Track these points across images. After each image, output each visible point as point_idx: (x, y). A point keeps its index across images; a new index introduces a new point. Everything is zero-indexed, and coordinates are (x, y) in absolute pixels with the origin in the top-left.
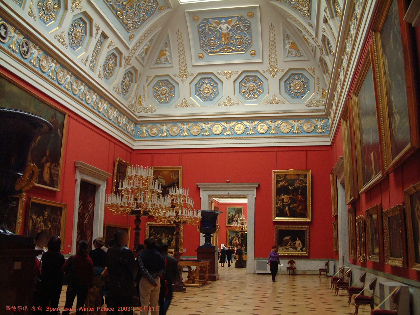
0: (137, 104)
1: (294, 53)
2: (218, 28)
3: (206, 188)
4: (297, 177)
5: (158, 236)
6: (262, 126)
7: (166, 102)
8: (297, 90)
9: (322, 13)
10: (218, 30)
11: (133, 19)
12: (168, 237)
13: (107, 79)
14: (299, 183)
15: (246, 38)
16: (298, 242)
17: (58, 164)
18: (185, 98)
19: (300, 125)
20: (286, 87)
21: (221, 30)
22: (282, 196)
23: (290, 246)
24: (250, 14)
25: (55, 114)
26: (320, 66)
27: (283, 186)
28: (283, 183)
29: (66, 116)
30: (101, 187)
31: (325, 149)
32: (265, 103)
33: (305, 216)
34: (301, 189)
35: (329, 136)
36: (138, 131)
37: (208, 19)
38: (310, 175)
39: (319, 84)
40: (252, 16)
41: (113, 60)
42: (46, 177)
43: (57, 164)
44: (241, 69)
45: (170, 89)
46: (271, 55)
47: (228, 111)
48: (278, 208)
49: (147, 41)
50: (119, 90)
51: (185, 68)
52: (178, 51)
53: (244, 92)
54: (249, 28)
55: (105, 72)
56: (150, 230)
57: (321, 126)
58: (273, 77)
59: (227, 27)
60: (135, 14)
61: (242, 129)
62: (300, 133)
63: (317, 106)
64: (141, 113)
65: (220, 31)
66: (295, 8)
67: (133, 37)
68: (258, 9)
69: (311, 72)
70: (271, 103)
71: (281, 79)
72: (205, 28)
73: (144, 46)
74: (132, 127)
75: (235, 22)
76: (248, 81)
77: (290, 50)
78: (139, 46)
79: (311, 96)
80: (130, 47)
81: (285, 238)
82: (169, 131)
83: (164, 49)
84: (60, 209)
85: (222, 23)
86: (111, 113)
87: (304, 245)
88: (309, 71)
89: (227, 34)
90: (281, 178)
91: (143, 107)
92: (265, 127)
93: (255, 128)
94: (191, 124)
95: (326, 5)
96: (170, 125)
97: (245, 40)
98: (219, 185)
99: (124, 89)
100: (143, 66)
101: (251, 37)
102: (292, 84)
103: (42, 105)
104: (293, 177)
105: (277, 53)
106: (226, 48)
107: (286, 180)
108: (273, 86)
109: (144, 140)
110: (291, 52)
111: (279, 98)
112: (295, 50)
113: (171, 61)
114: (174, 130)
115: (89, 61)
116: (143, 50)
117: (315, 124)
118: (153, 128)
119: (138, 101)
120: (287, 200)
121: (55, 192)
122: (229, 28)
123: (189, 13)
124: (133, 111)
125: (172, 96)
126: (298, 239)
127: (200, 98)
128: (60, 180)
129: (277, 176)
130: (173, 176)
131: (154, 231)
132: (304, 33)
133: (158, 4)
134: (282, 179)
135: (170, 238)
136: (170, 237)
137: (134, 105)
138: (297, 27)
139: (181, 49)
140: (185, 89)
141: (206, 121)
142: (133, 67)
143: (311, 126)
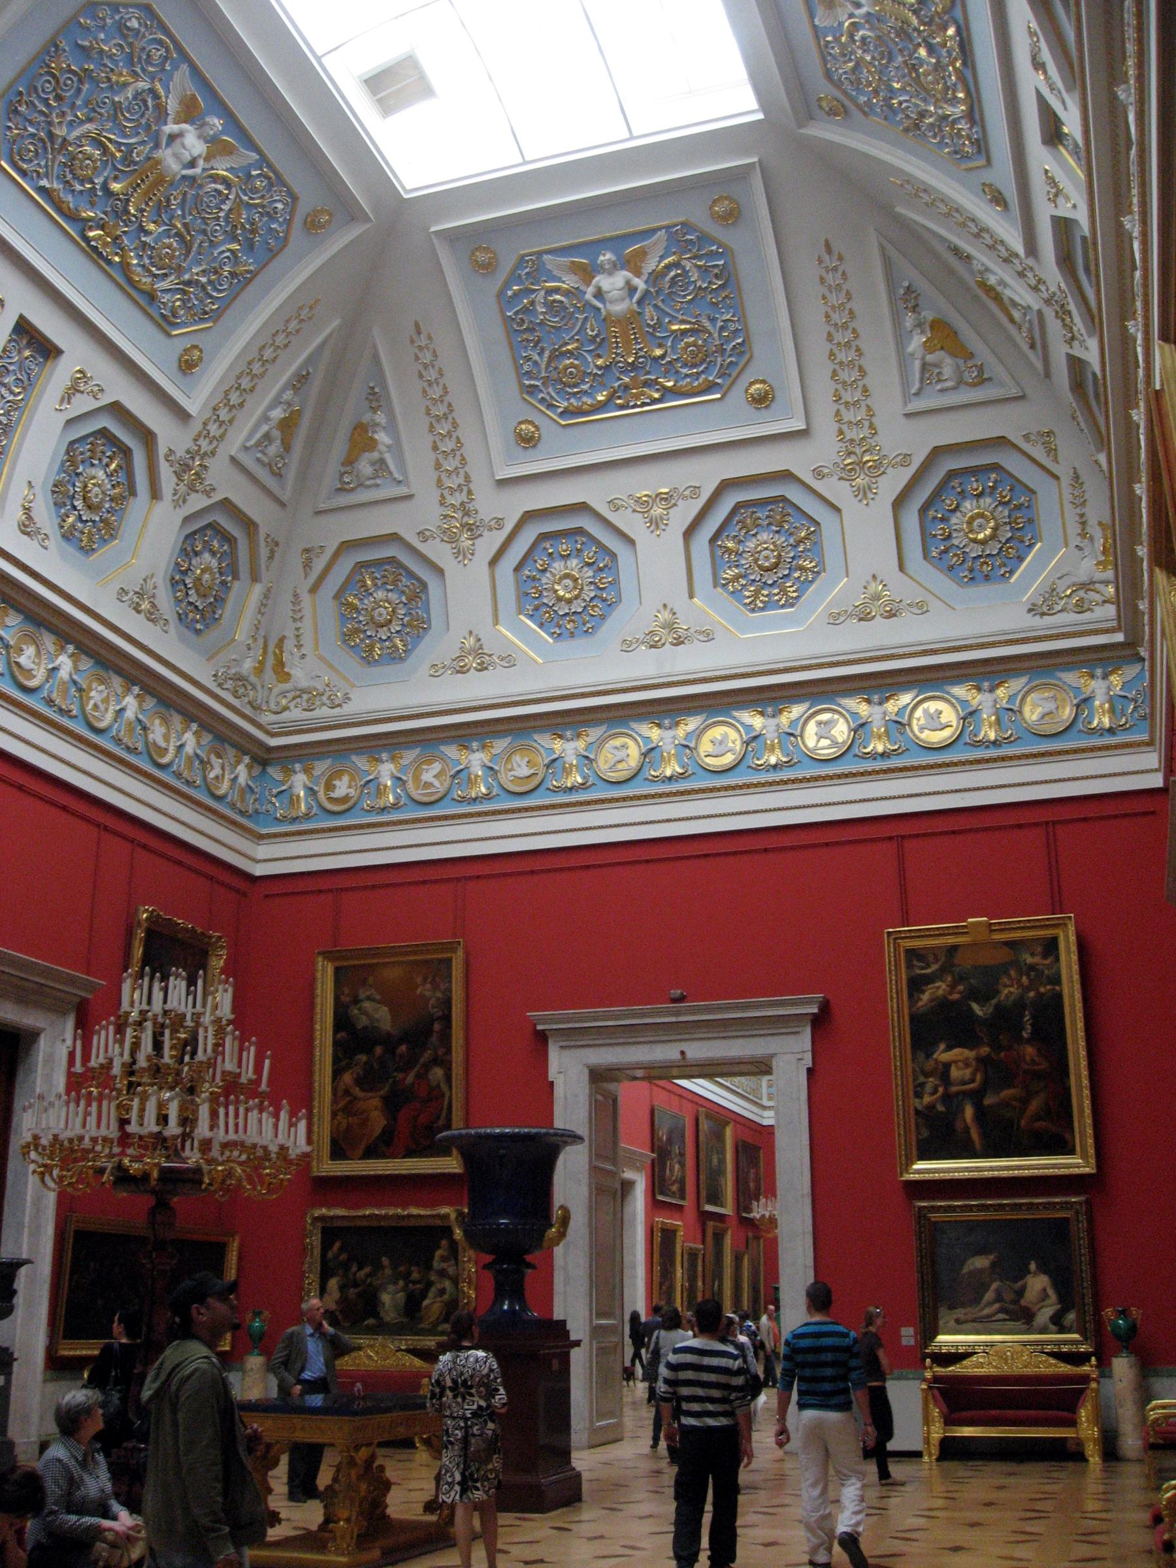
0: (269, 674)
2: (589, 296)
3: (575, 1036)
4: (1003, 955)
5: (362, 1273)
6: (826, 723)
7: (395, 657)
8: (983, 542)
9: (1029, 81)
10: (587, 304)
11: (179, 270)
12: (406, 1276)
13: (88, 551)
14: (1020, 985)
15: (722, 328)
16: (1037, 1283)
18: (475, 632)
19: (1004, 704)
21: (604, 303)
22: (943, 1055)
23: (997, 1306)
26: (1078, 413)
27: (943, 1005)
28: (941, 988)
30: (43, 1042)
31: (1137, 806)
32: (835, 619)
33: (1063, 1146)
34: (1033, 1017)
35: (1150, 743)
36: (275, 791)
37: (540, 254)
38: (1073, 938)
39: (1084, 504)
40: (732, 216)
41: (113, 466)
44: (708, 474)
45: (410, 600)
46: (842, 393)
47: (667, 669)
50: (154, 605)
51: (463, 497)
52: (426, 421)
53: (736, 578)
54: (728, 277)
55: (71, 520)
56: (326, 1247)
57: (1111, 700)
58: (863, 493)
59: (628, 283)
60: (187, 246)
61: (730, 744)
62: (1009, 741)
63: (1081, 608)
64: (285, 716)
65: (600, 305)
67: (200, 359)
69: (1038, 453)
70: (865, 618)
71: (899, 503)
72: (532, 303)
74: (242, 771)
75: (662, 258)
76: (749, 530)
77: (929, 358)
78: (241, 405)
80: (193, 406)
81: (970, 1262)
82: (404, 782)
83: (367, 417)
85: (600, 269)
86: (106, 701)
87: (1067, 1301)
89: (632, 319)
90: (928, 966)
91: (296, 689)
92: (841, 731)
93: (792, 735)
94: (500, 745)
96: (409, 756)
97: (716, 335)
98: (634, 1015)
99: (190, 603)
100: (283, 505)
101: (743, 319)
102: (954, 520)
104: (986, 958)
106: (635, 383)
107: (957, 970)
108: (864, 537)
109: (299, 833)
110: (936, 365)
111: (899, 588)
112: (953, 354)
113: (404, 471)
114: (427, 777)
116: (265, 428)
118: (338, 774)
119: (270, 661)
120: (967, 1073)
122: (636, 289)
123: (453, 237)
124: (248, 711)
125: (418, 627)
126: (1033, 1266)
127: (541, 626)
129: (913, 955)
130: (428, 986)
131: (341, 1249)
132: (982, 258)
133: (295, 199)
134: (934, 967)
135: (414, 1283)
136: (415, 1275)
137: (253, 679)
138: (943, 239)
139: (441, 410)
140: (469, 593)
141: (567, 725)
142: (226, 505)
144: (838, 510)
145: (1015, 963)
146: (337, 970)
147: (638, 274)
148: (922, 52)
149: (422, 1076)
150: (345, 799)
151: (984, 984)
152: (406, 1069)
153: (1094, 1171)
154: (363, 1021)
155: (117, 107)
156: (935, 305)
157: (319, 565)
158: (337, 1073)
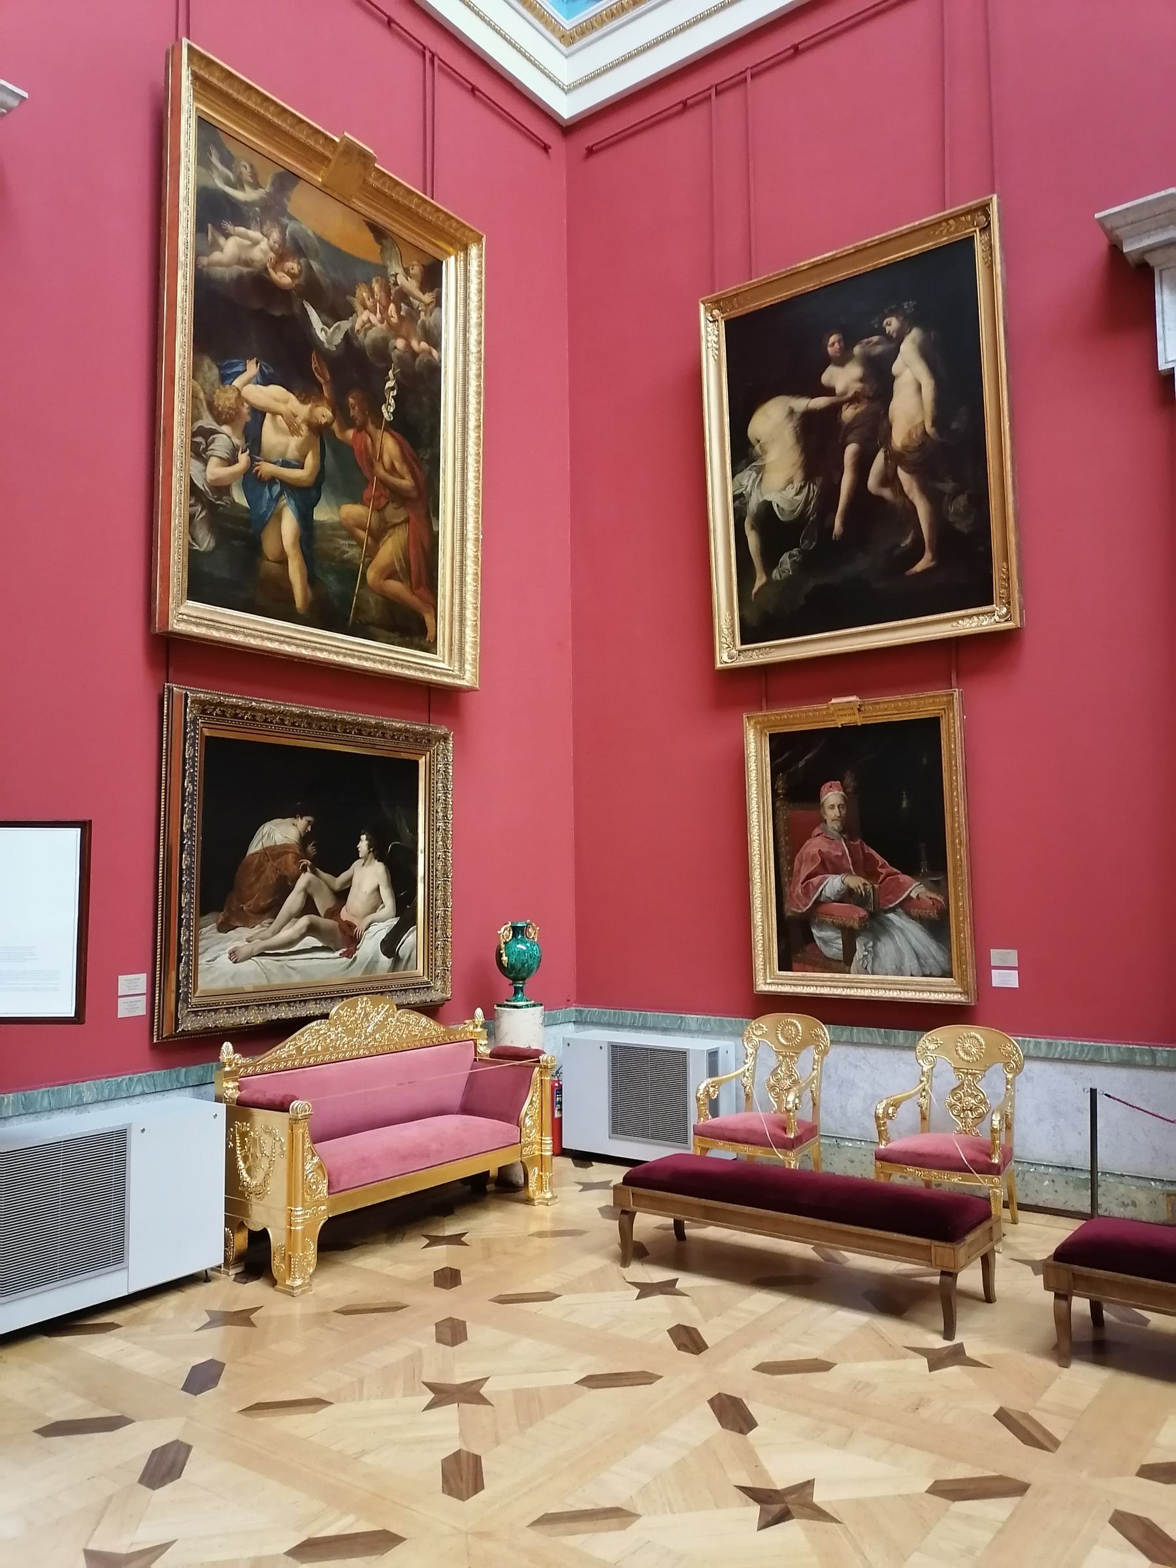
81: (266, 828)
126: (363, 845)
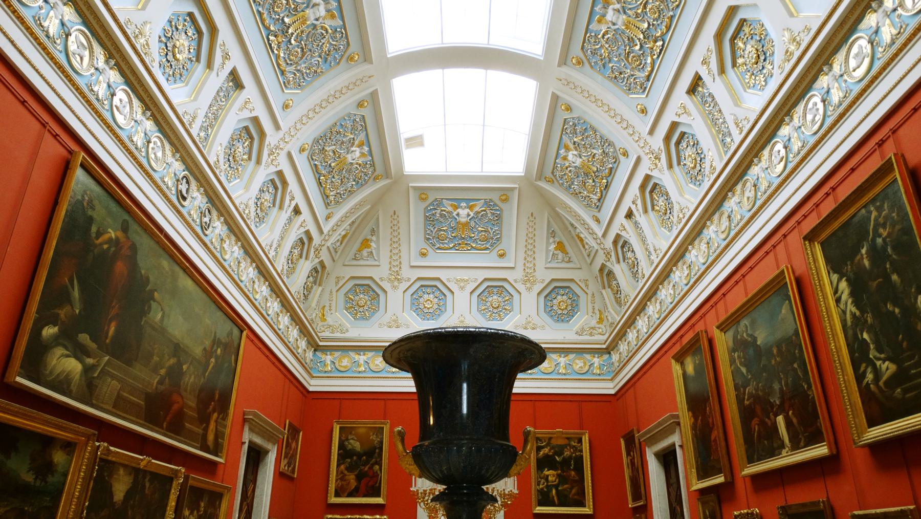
0: (318, 319)
1: (560, 256)
4: (566, 441)
17: (227, 415)
20: (546, 305)
22: (546, 472)
24: (503, 198)
25: (231, 330)
28: (546, 450)
29: (245, 333)
33: (582, 505)
40: (506, 200)
42: (211, 437)
43: (225, 418)
44: (482, 275)
48: (540, 492)
49: (346, 225)
54: (499, 217)
58: (529, 289)
60: (342, 182)
63: (591, 335)
66: (576, 194)
68: (516, 192)
71: (539, 294)
73: (341, 231)
79: (582, 319)
80: (325, 231)
84: (220, 496)
88: (580, 283)
89: (467, 224)
95: (638, 195)
103: (220, 313)
104: (561, 442)
105: (535, 255)
115: (273, 248)
117: (590, 361)
121: (215, 464)
123: (415, 188)
128: (226, 444)
132: (580, 228)
139: (396, 240)
142: (322, 263)
143: (585, 363)
144: (520, 293)
145: (569, 445)
146: (340, 428)
147: (472, 211)
148: (591, 181)
149: (371, 468)
150: (344, 367)
151: (559, 451)
152: (365, 465)
153: (591, 513)
154: (350, 447)
155: (343, 143)
156: (561, 236)
157: (340, 284)
158: (338, 466)
